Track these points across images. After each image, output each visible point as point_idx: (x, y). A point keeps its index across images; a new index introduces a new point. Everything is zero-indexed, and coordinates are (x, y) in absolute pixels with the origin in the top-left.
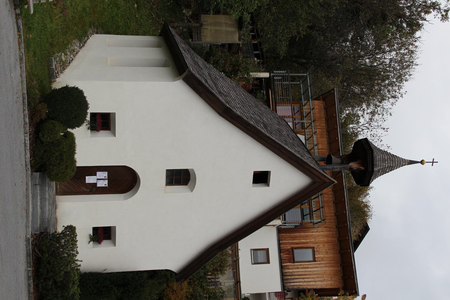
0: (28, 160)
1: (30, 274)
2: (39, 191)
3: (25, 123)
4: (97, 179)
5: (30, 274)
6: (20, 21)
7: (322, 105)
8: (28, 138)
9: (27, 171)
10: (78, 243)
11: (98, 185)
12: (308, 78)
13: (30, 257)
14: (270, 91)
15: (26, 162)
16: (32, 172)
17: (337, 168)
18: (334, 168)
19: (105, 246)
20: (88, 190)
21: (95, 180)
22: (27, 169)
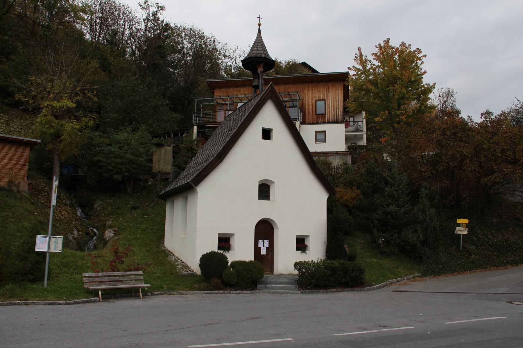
0: (249, 292)
1: (324, 291)
2: (270, 286)
3: (224, 293)
6: (156, 293)
7: (218, 90)
8: (234, 292)
9: (256, 293)
10: (306, 261)
11: (268, 246)
12: (199, 99)
14: (207, 126)
15: (250, 293)
16: (257, 289)
17: (262, 82)
18: (262, 84)
19: (310, 243)
20: (271, 253)
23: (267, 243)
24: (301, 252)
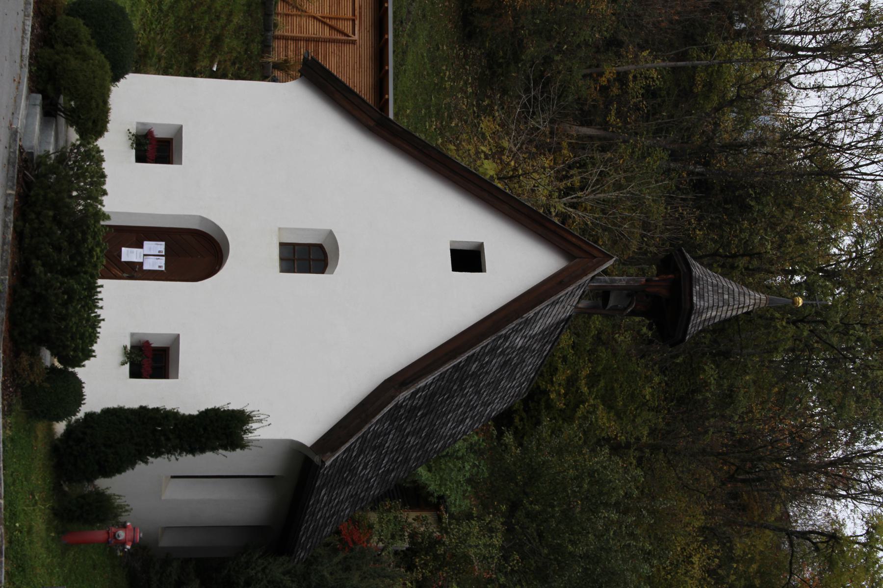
0: (27, 53)
4: (145, 255)
5: (10, 203)
11: (146, 267)
13: (14, 166)
15: (22, 56)
16: (31, 90)
17: (621, 280)
18: (615, 281)
21: (140, 257)
22: (23, 66)
23: (157, 264)
24: (125, 348)
